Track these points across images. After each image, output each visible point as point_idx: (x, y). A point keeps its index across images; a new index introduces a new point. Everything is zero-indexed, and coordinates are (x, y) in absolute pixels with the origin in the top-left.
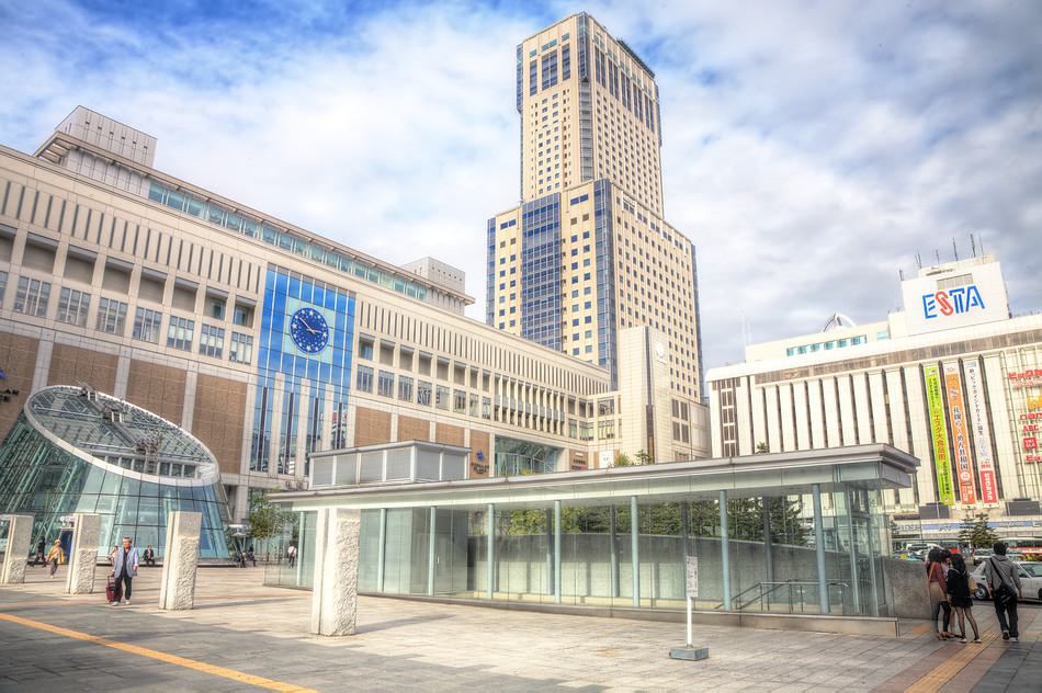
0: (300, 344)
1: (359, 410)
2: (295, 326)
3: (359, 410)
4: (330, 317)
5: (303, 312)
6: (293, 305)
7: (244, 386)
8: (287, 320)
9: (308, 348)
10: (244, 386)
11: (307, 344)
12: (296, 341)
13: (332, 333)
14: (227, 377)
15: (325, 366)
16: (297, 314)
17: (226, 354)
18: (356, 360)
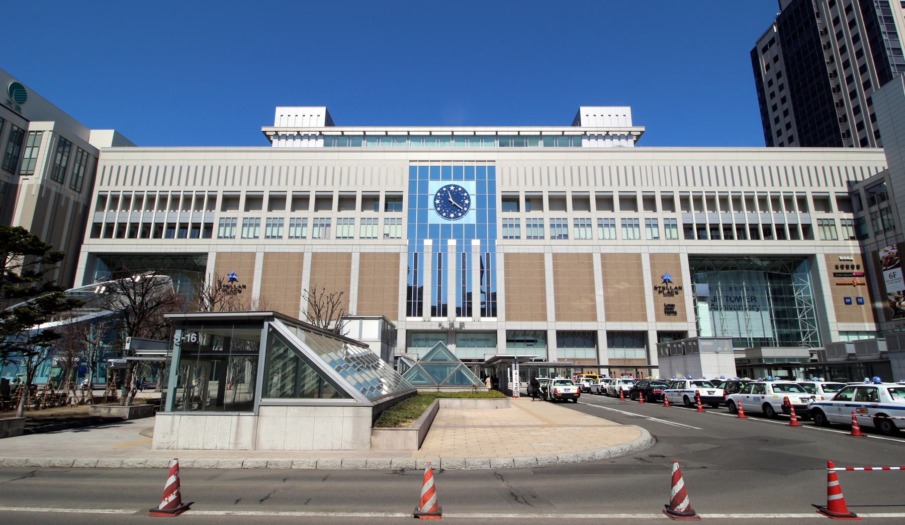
0: (444, 214)
1: (507, 256)
2: (437, 202)
3: (507, 256)
4: (470, 187)
5: (444, 189)
6: (434, 186)
7: (397, 256)
8: (431, 200)
9: (452, 215)
10: (397, 256)
11: (450, 212)
12: (440, 213)
13: (473, 199)
14: (383, 251)
15: (469, 227)
16: (438, 192)
17: (381, 236)
18: (501, 215)
